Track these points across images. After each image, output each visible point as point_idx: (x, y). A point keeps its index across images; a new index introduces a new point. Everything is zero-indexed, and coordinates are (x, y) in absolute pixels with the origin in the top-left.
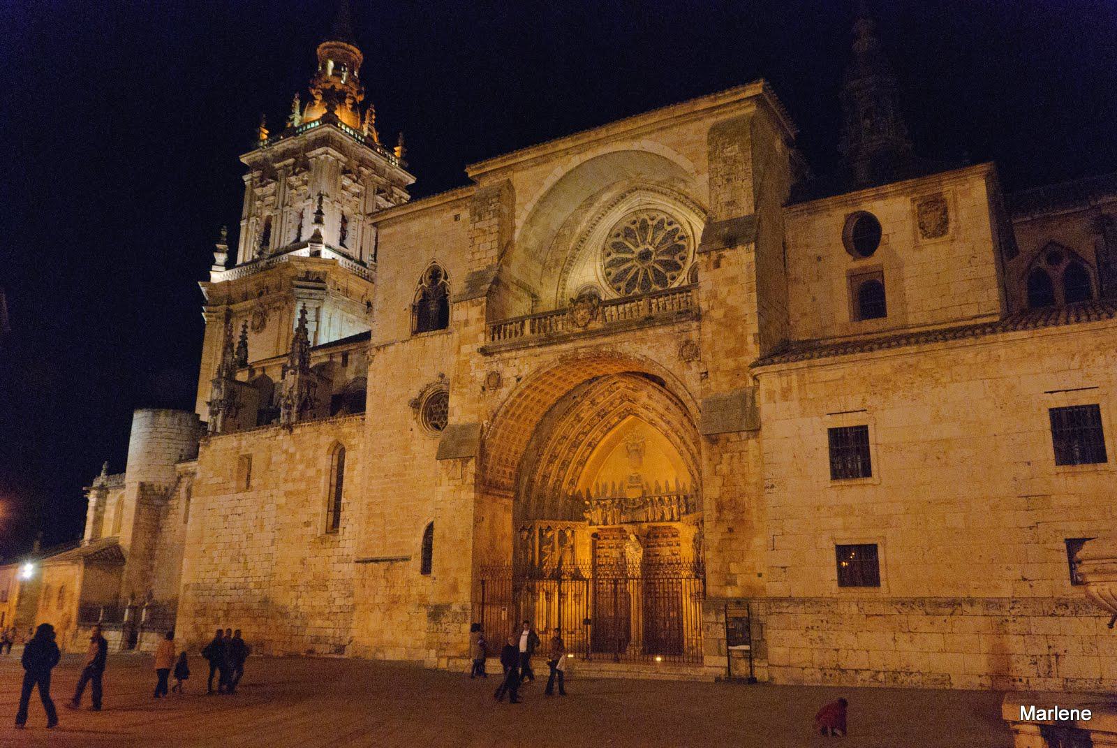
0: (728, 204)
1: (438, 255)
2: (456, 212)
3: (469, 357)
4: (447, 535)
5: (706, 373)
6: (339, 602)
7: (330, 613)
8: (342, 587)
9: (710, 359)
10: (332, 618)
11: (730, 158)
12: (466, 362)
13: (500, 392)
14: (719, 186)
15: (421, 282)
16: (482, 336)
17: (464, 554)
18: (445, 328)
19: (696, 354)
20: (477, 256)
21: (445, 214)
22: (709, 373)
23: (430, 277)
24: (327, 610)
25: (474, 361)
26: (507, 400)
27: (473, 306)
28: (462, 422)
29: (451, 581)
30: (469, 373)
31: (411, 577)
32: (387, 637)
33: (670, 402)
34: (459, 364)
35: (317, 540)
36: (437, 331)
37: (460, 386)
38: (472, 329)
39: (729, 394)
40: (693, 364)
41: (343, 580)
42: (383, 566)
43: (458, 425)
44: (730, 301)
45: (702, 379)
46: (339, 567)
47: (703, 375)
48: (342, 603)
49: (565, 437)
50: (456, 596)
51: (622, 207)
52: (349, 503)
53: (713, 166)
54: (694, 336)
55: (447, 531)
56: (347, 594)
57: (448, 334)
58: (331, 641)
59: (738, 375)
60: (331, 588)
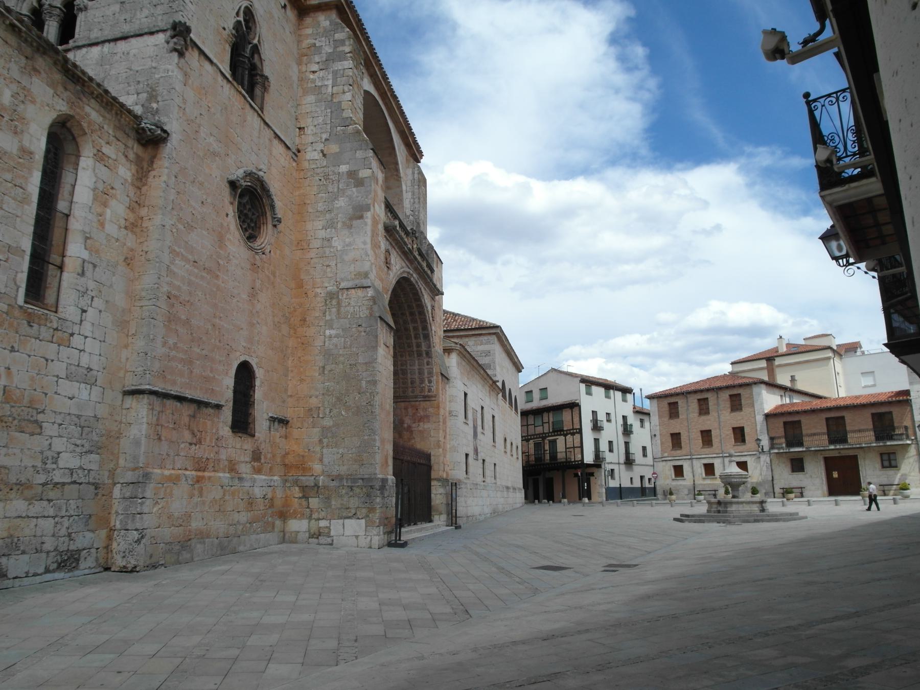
6: (68, 460)
7: (43, 485)
8: (75, 431)
10: (52, 495)
15: (238, 14)
24: (41, 478)
31: (221, 433)
32: (195, 524)
35: (17, 313)
41: (79, 417)
42: (186, 410)
46: (67, 388)
48: (74, 463)
52: (95, 266)
56: (87, 447)
58: (49, 545)
60: (50, 429)
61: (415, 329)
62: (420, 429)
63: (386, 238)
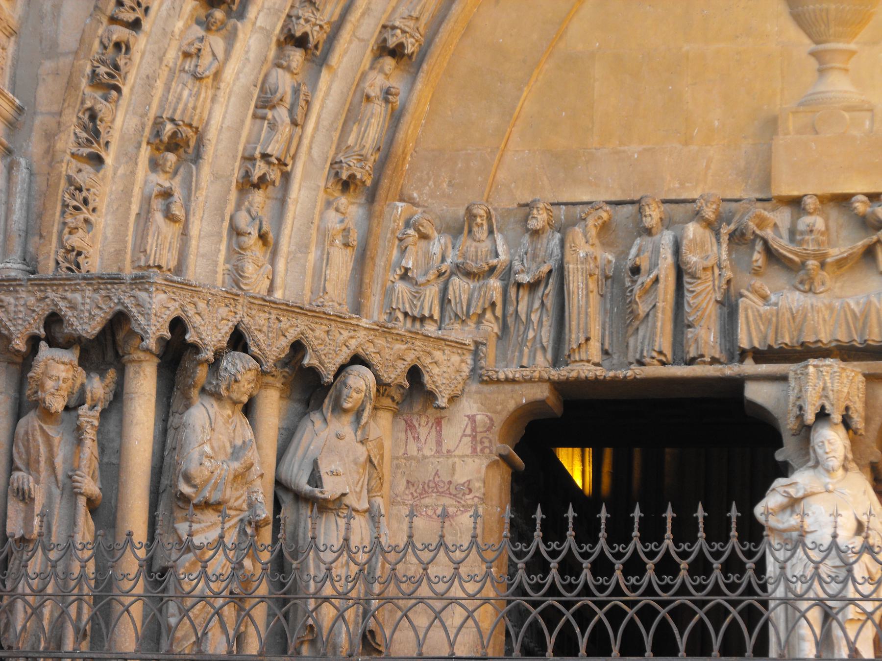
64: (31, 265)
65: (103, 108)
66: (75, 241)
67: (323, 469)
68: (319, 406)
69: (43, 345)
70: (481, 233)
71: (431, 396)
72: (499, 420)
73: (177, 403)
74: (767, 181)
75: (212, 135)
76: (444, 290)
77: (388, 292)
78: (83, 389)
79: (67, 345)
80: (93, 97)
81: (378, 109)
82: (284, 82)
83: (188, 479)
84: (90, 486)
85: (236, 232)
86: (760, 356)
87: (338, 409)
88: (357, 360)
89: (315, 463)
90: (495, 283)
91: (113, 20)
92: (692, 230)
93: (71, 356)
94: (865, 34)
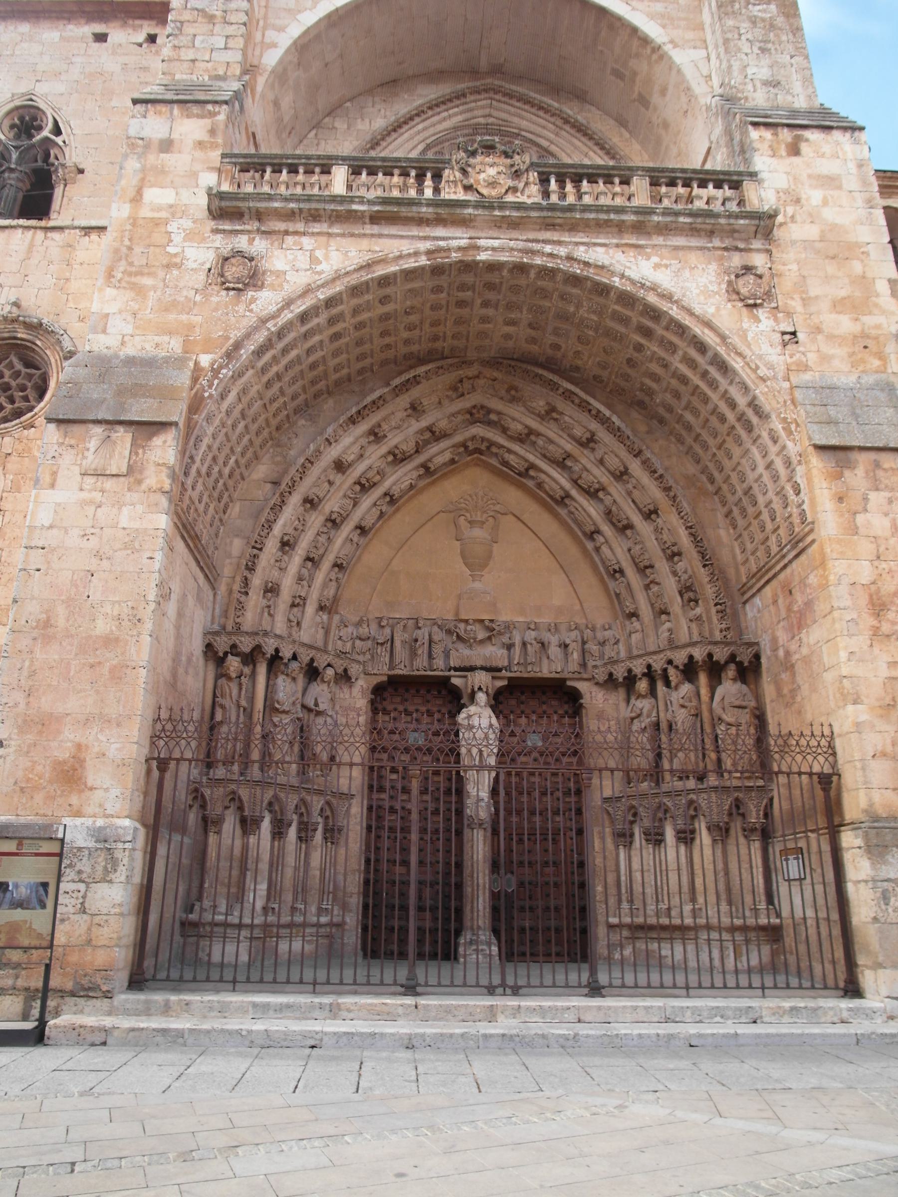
0: (766, 83)
1: (41, 89)
2: (99, 28)
3: (164, 214)
4: (61, 622)
5: (794, 334)
9: (799, 309)
11: (763, 20)
12: (157, 223)
13: (253, 300)
14: (746, 54)
16: (209, 179)
17: (118, 674)
18: (41, 219)
19: (768, 295)
20: (190, 54)
21: (71, 27)
22: (800, 336)
23: (12, 127)
25: (187, 224)
26: (273, 317)
27: (188, 117)
28: (130, 351)
29: (63, 754)
30: (164, 247)
33: (594, 425)
34: (134, 225)
36: (22, 222)
37: (134, 269)
38: (177, 161)
39: (853, 378)
40: (761, 313)
43: (117, 356)
44: (829, 214)
45: (785, 344)
47: (787, 337)
49: (340, 466)
50: (74, 800)
51: (456, 114)
53: (730, 23)
54: (759, 261)
55: (61, 611)
57: (46, 229)
59: (865, 347)
61: (692, 364)
62: (805, 651)
63: (224, 231)
64: (224, 628)
65: (249, 576)
66: (238, 620)
67: (319, 701)
68: (315, 680)
69: (230, 656)
70: (365, 626)
71: (350, 678)
72: (371, 688)
73: (272, 676)
74: (457, 614)
75: (282, 588)
76: (354, 643)
77: (334, 644)
78: (242, 671)
79: (236, 655)
80: (246, 573)
81: (334, 583)
82: (305, 572)
83: (278, 703)
84: (244, 703)
85: (290, 621)
86: (456, 669)
87: (323, 681)
88: (329, 665)
89: (316, 700)
90: (370, 642)
91: (254, 547)
92: (435, 628)
93: (238, 659)
94: (486, 570)
